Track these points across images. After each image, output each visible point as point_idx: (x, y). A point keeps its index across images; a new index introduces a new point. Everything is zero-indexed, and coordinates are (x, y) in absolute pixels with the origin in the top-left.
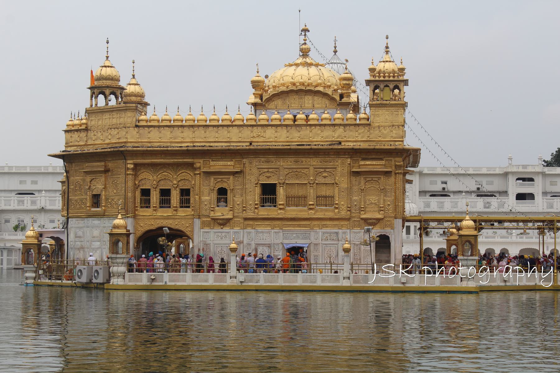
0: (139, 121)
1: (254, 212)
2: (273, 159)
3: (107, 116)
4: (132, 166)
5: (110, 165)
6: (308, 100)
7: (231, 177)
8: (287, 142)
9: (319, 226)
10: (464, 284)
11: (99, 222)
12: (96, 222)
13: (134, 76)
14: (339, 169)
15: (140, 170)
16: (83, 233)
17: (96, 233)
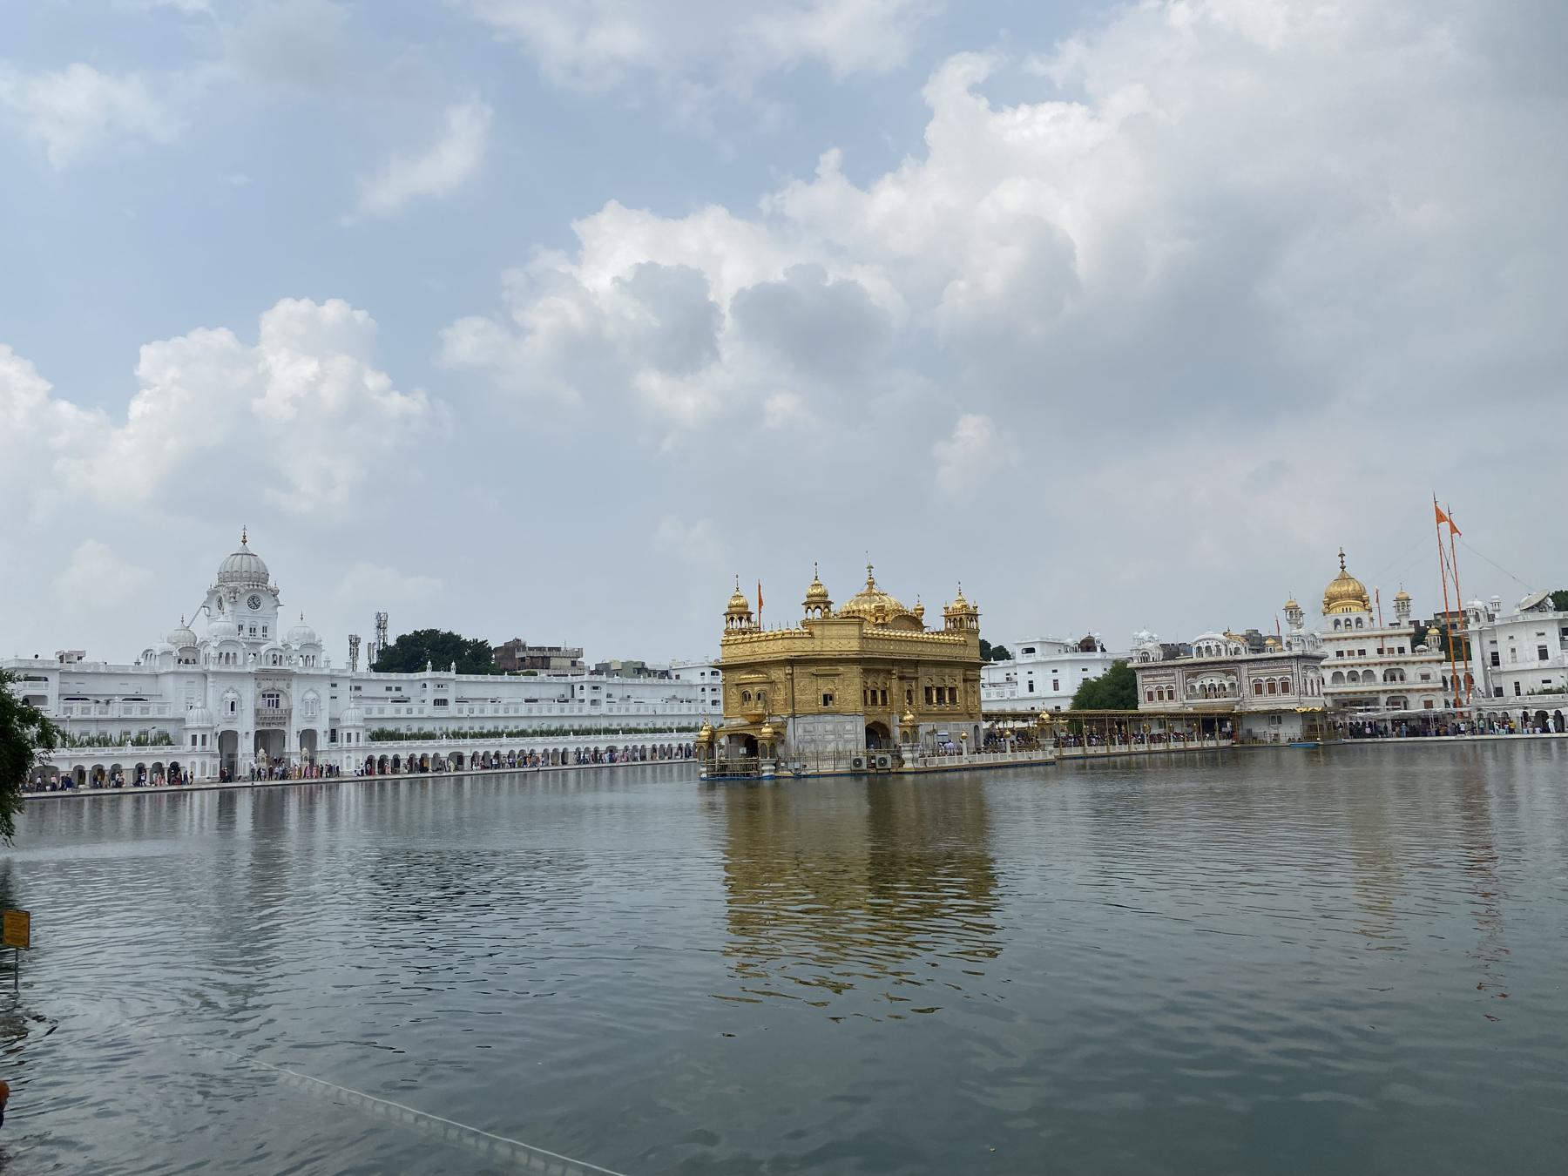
5: (841, 669)
12: (829, 718)
17: (829, 727)
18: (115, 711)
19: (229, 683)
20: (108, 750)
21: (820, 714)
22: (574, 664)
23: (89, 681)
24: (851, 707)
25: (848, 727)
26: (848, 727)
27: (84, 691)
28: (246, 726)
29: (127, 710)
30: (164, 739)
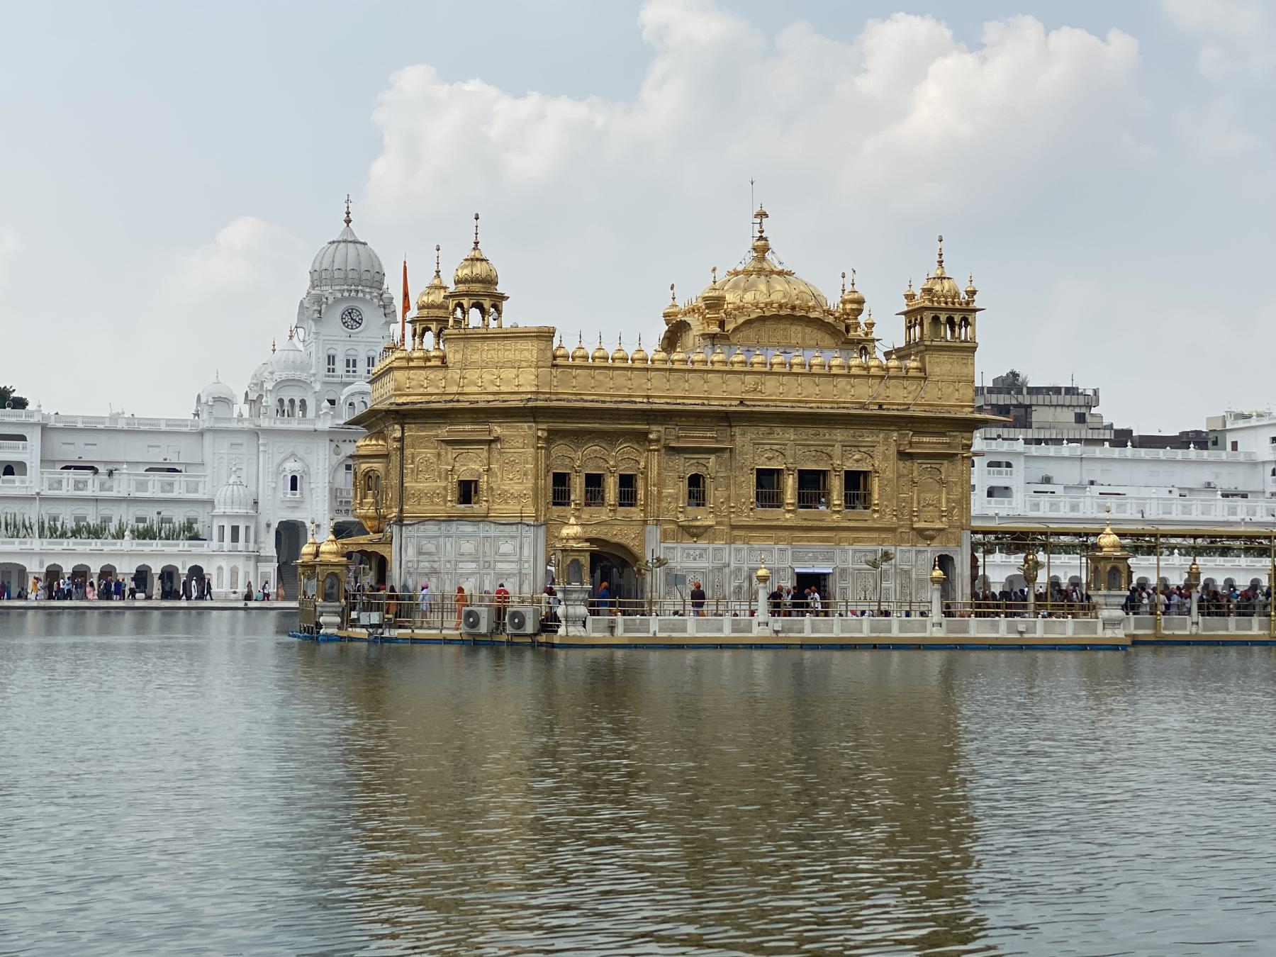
0: (555, 357)
1: (748, 516)
2: (779, 430)
3: (495, 345)
4: (546, 434)
5: (498, 430)
6: (796, 333)
7: (713, 458)
8: (799, 401)
9: (847, 539)
10: (1109, 634)
11: (475, 529)
12: (468, 528)
13: (438, 272)
14: (881, 448)
15: (554, 441)
16: (437, 547)
17: (467, 547)
18: (121, 487)
19: (288, 446)
20: (95, 544)
21: (450, 519)
22: (1080, 419)
23: (80, 440)
24: (512, 508)
25: (506, 548)
26: (506, 548)
27: (89, 456)
28: (317, 513)
29: (142, 486)
30: (191, 533)
